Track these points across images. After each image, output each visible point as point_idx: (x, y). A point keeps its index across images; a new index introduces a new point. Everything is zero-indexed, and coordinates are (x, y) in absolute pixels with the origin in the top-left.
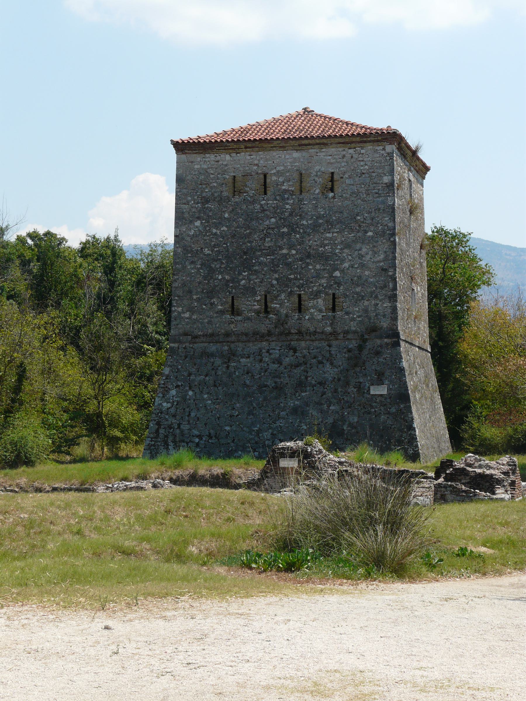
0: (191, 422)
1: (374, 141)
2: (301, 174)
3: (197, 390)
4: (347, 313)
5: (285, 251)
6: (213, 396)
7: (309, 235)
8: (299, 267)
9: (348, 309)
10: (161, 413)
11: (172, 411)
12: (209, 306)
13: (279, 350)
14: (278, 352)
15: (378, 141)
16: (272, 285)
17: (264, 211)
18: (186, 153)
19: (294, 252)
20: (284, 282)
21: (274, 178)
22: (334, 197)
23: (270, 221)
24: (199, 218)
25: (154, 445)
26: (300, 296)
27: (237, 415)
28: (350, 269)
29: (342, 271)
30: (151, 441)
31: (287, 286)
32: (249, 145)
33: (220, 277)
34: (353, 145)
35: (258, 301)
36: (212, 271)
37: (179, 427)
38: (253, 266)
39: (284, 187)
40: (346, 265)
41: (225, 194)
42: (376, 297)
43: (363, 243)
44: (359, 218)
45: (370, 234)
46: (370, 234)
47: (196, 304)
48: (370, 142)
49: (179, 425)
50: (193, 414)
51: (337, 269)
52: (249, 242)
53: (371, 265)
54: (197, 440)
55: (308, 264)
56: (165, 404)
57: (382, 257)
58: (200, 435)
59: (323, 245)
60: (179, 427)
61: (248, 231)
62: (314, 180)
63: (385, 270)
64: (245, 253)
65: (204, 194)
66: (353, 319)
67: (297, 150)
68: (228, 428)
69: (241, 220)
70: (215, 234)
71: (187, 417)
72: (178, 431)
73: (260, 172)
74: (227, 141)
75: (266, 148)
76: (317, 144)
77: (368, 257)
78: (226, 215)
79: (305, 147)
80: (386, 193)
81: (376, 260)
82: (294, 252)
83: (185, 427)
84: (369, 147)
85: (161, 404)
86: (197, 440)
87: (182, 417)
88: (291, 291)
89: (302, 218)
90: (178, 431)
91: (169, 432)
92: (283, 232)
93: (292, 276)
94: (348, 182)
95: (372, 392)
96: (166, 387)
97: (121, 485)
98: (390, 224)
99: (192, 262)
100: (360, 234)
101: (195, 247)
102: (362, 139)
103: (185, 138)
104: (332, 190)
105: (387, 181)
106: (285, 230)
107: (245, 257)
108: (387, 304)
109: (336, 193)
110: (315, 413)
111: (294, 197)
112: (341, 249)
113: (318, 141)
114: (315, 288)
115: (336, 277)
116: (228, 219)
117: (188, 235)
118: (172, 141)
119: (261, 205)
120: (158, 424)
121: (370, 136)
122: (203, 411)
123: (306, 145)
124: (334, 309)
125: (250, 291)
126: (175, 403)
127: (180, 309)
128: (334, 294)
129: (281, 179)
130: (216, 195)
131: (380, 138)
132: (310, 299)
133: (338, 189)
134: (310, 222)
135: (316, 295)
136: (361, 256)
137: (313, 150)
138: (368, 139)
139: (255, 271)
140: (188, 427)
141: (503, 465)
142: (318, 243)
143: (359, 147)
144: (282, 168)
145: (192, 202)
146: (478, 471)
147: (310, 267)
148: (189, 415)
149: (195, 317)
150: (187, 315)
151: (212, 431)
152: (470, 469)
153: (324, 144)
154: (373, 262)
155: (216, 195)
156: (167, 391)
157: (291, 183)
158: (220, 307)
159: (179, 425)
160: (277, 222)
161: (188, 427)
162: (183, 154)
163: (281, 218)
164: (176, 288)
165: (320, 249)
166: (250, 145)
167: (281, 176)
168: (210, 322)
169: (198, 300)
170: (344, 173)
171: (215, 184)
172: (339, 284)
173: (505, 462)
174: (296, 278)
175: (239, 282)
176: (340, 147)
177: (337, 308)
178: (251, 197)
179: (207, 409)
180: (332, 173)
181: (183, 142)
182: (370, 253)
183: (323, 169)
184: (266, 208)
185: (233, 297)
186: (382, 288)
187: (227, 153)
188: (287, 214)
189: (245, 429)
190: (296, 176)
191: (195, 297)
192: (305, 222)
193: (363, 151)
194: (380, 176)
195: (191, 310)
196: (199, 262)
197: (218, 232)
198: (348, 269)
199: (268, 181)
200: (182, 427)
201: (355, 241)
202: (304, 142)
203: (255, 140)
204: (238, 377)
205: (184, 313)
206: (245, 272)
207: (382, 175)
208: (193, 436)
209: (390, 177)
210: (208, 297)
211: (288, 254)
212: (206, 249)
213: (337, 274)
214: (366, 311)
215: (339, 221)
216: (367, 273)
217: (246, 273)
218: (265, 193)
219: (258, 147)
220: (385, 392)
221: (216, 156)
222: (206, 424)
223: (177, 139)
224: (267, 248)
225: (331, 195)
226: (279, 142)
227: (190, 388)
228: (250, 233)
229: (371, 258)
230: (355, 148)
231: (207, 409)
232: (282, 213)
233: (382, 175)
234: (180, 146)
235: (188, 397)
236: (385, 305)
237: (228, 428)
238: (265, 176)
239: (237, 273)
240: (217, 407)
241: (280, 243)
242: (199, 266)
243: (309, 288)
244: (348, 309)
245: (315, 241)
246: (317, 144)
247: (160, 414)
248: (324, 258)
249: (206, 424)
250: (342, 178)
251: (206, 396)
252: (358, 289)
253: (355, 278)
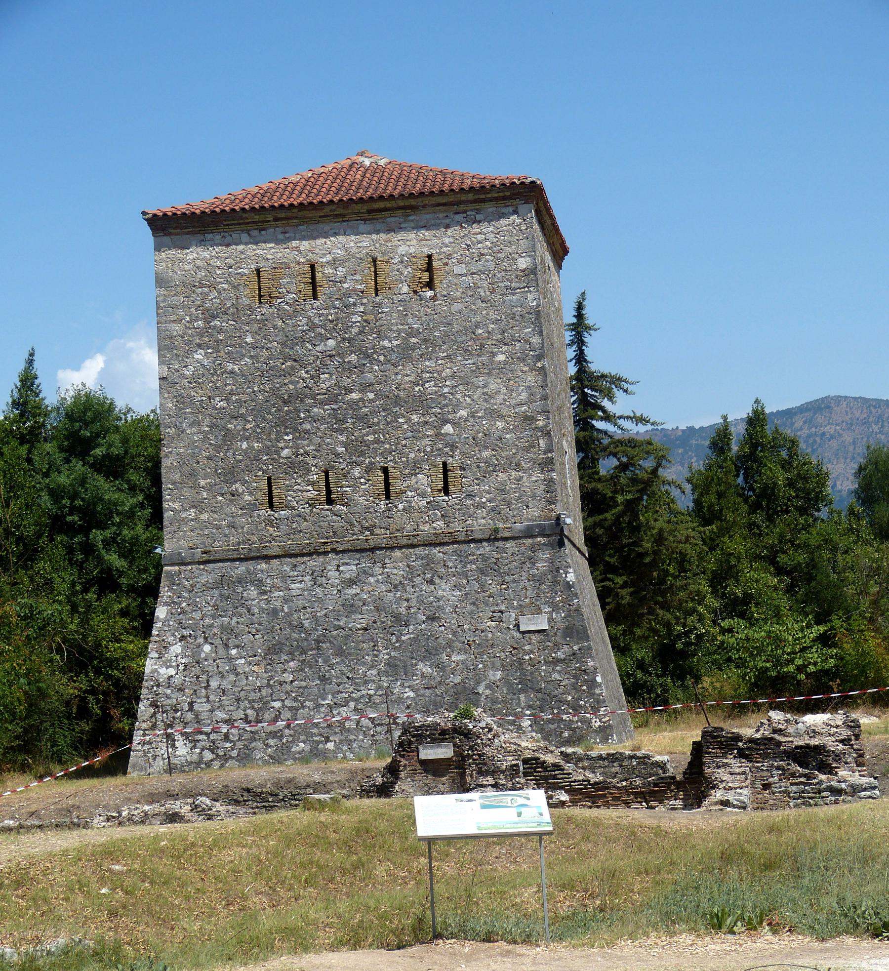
0: (212, 697)
1: (497, 199)
2: (375, 261)
3: (218, 642)
4: (470, 496)
5: (355, 396)
6: (247, 651)
7: (395, 366)
8: (382, 422)
9: (471, 489)
10: (158, 686)
11: (177, 680)
12: (229, 496)
13: (357, 565)
14: (354, 568)
15: (504, 198)
16: (337, 455)
17: (313, 327)
18: (170, 234)
19: (371, 396)
20: (357, 449)
21: (328, 270)
22: (434, 298)
23: (325, 345)
24: (199, 346)
25: (150, 743)
26: (385, 470)
27: (292, 682)
28: (471, 419)
29: (456, 424)
30: (144, 735)
31: (362, 454)
32: (282, 215)
33: (245, 445)
34: (462, 207)
35: (313, 484)
36: (229, 437)
37: (191, 708)
38: (301, 424)
39: (346, 285)
40: (463, 413)
41: (247, 302)
42: (518, 465)
43: (489, 374)
44: (480, 331)
45: (501, 358)
46: (501, 358)
47: (205, 494)
48: (490, 200)
49: (191, 704)
50: (214, 684)
51: (447, 422)
52: (291, 382)
53: (504, 412)
54: (224, 729)
55: (397, 416)
56: (163, 671)
57: (524, 396)
58: (230, 720)
60: (191, 708)
61: (289, 364)
62: (398, 270)
63: (528, 419)
64: (285, 402)
65: (208, 305)
66: (482, 506)
67: (365, 220)
68: (277, 704)
69: (275, 344)
70: (232, 372)
71: (203, 691)
72: (190, 716)
73: (302, 260)
74: (243, 209)
75: (311, 218)
76: (400, 208)
77: (500, 398)
78: (249, 339)
79: (379, 215)
80: (524, 288)
81: (513, 402)
82: (371, 396)
83: (202, 707)
84: (491, 210)
85: (156, 670)
86: (224, 729)
87: (195, 691)
88: (371, 463)
89: (381, 336)
90: (190, 716)
91: (174, 718)
92: (349, 362)
93: (370, 438)
94: (458, 269)
95: (522, 628)
96: (163, 640)
97: (135, 813)
98: (535, 340)
99: (192, 424)
100: (483, 358)
101: (198, 396)
102: (477, 197)
103: (167, 209)
104: (430, 285)
105: (524, 267)
106: (353, 358)
107: (286, 408)
108: (538, 476)
109: (438, 290)
110: (427, 670)
111: (365, 301)
112: (453, 387)
113: (401, 203)
114: (412, 455)
115: (447, 434)
116: (254, 346)
117: (184, 377)
118: (144, 213)
119: (309, 318)
120: (154, 705)
121: (490, 191)
122: (232, 677)
123: (380, 210)
124: (446, 490)
125: (297, 466)
126: (181, 668)
127: (177, 506)
128: (445, 464)
129: (341, 271)
130: (228, 304)
131: (507, 193)
132: (405, 477)
133: (441, 287)
134: (396, 343)
135: (416, 468)
136: (488, 397)
137: (393, 219)
138: (489, 196)
139: (307, 432)
140: (207, 706)
141: (837, 727)
142: (411, 378)
143: (472, 210)
144: (342, 252)
145: (188, 319)
146: (799, 742)
147: (401, 420)
148: (207, 686)
149: (204, 516)
150: (192, 513)
151: (249, 712)
152: (783, 739)
153: (413, 208)
154: (509, 407)
155: (228, 304)
156: (164, 647)
157: (358, 277)
158: (247, 498)
159: (191, 704)
160: (338, 344)
161: (207, 706)
162: (165, 235)
163: (344, 339)
164: (170, 468)
165: (417, 389)
166: (283, 215)
167: (340, 265)
168: (232, 526)
169: (209, 488)
170: (449, 256)
171: (225, 286)
172: (453, 447)
173: (840, 723)
174: (377, 441)
175: (278, 453)
176: (440, 212)
177: (451, 488)
178: (290, 306)
179: (238, 674)
180: (430, 257)
181: (165, 215)
182: (504, 390)
183: (412, 250)
184: (316, 321)
185: (269, 479)
186: (527, 449)
187: (242, 231)
188: (355, 330)
189: (307, 703)
190: (367, 264)
191: (202, 483)
192: (386, 343)
194: (511, 258)
195: (197, 505)
196: (207, 422)
197: (236, 368)
198: (466, 420)
199: (319, 276)
200: (196, 707)
201: (476, 372)
202: (377, 205)
203: (292, 205)
204: (289, 614)
205: (185, 510)
206: (287, 434)
207: (516, 256)
208: (218, 722)
209: (529, 260)
210: (225, 482)
211: (362, 400)
212: (218, 399)
213: (448, 429)
214: (502, 491)
215: (446, 338)
216: (499, 424)
217: (290, 437)
218: (315, 297)
219: (296, 218)
220: (545, 626)
221: (224, 237)
222: (238, 700)
223: (152, 210)
224: (324, 391)
225: (429, 294)
226: (334, 207)
227: (206, 638)
228: (293, 368)
229: (505, 400)
230: (465, 212)
231: (238, 674)
232: (347, 329)
233: (516, 256)
234: (160, 223)
235: (203, 655)
236: (534, 478)
237: (277, 704)
238: (313, 267)
239: (273, 437)
240: (256, 668)
241: (346, 382)
242: (207, 429)
243: (401, 454)
244: (471, 489)
245: (407, 375)
246: (400, 208)
247: (155, 688)
248: (421, 403)
249: (238, 700)
250: (447, 264)
251: (234, 652)
252: (486, 454)
253: (480, 435)
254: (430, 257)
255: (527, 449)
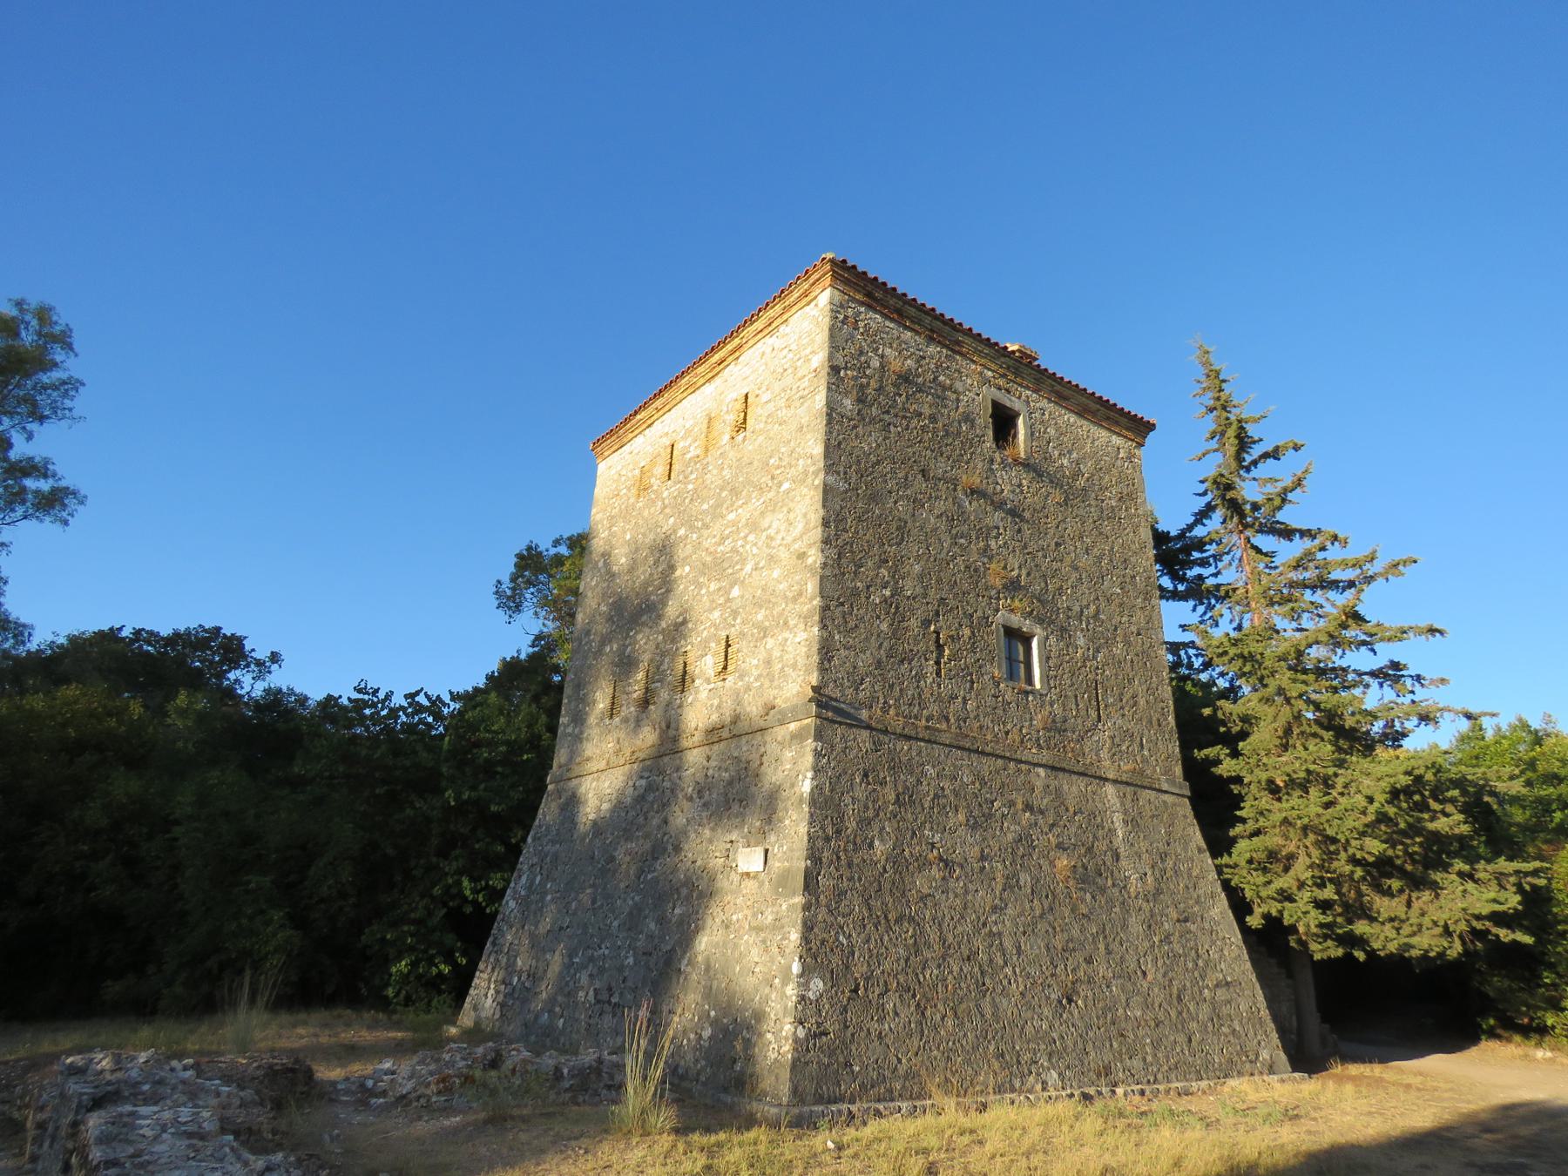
40: (748, 568)
45: (786, 486)
46: (786, 486)
53: (783, 554)
55: (699, 586)
59: (723, 539)
94: (764, 398)
172: (735, 613)
186: (795, 600)
193: (788, 330)
213: (736, 592)
214: (768, 662)
254: (747, 396)
255: (795, 600)
